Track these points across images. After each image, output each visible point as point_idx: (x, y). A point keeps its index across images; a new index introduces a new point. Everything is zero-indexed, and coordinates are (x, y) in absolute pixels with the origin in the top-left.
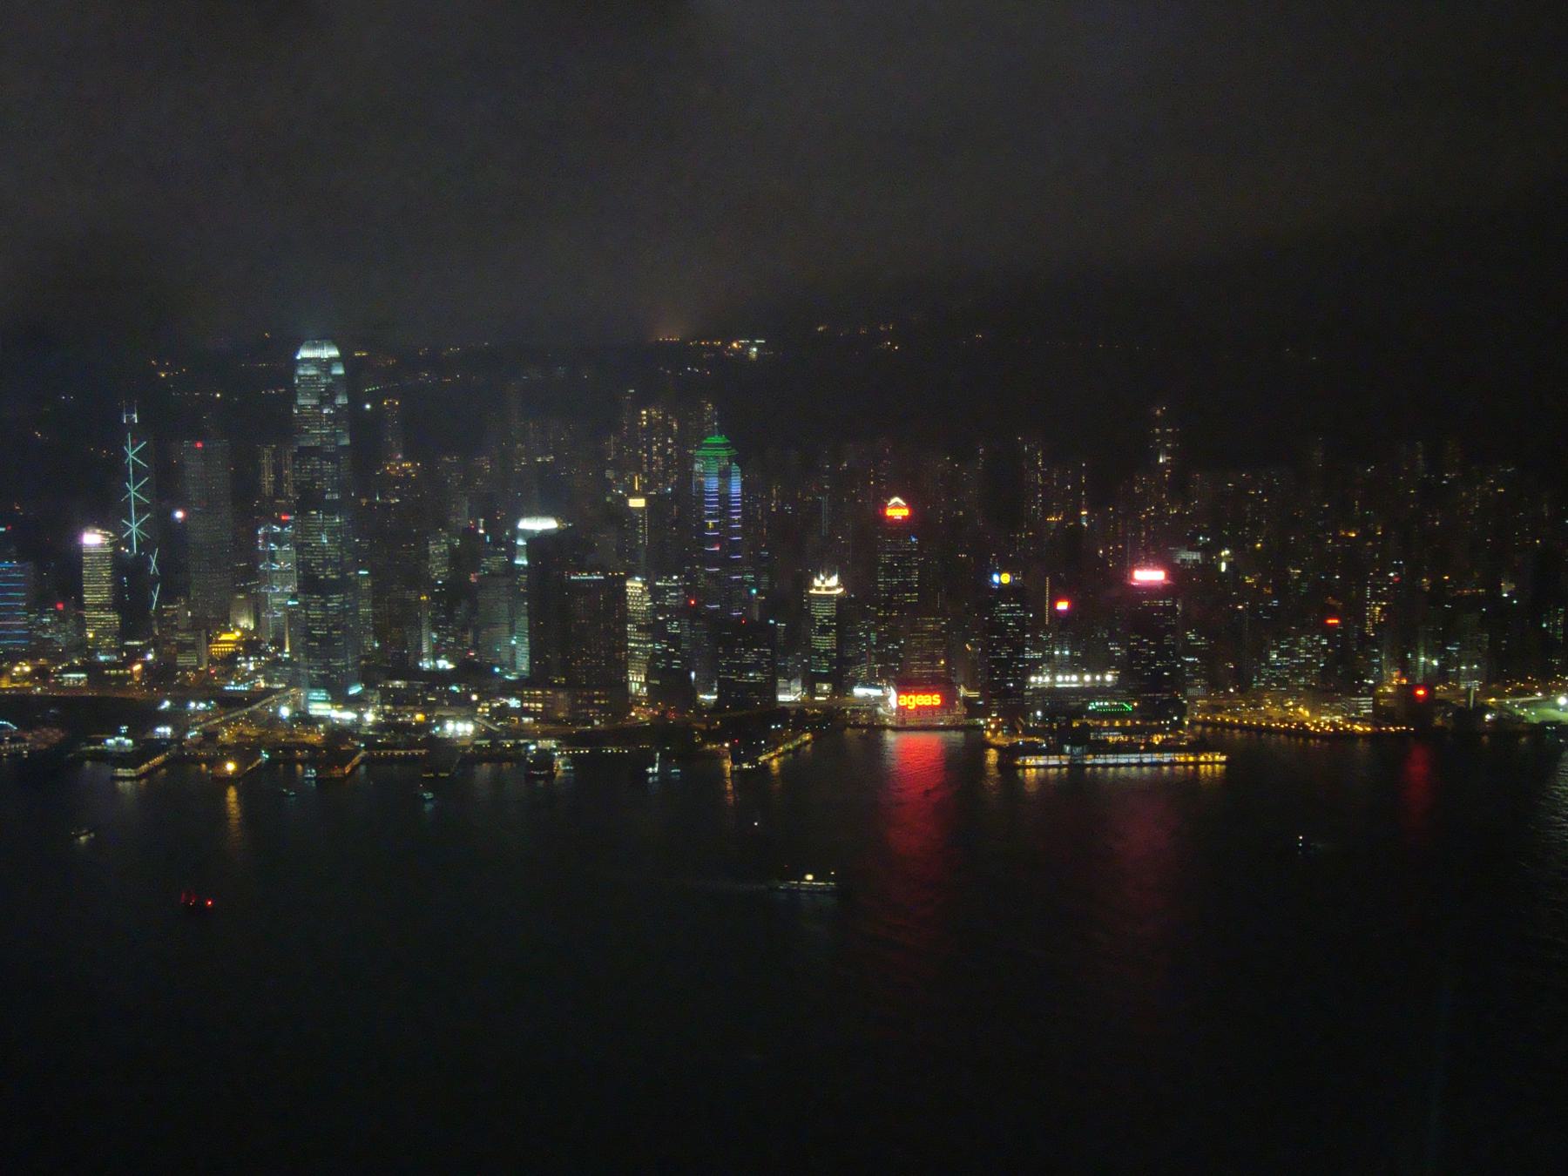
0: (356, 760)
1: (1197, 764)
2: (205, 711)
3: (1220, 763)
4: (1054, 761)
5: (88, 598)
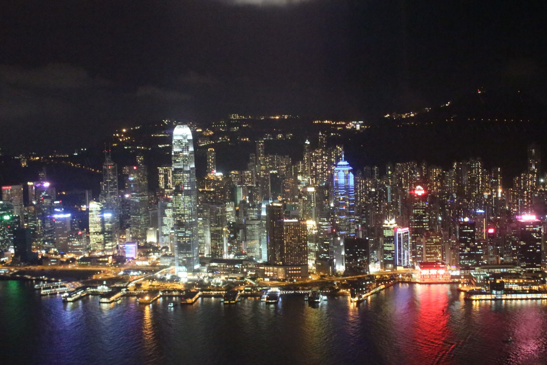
0: (197, 296)
2: (137, 275)
4: (489, 297)
5: (91, 230)
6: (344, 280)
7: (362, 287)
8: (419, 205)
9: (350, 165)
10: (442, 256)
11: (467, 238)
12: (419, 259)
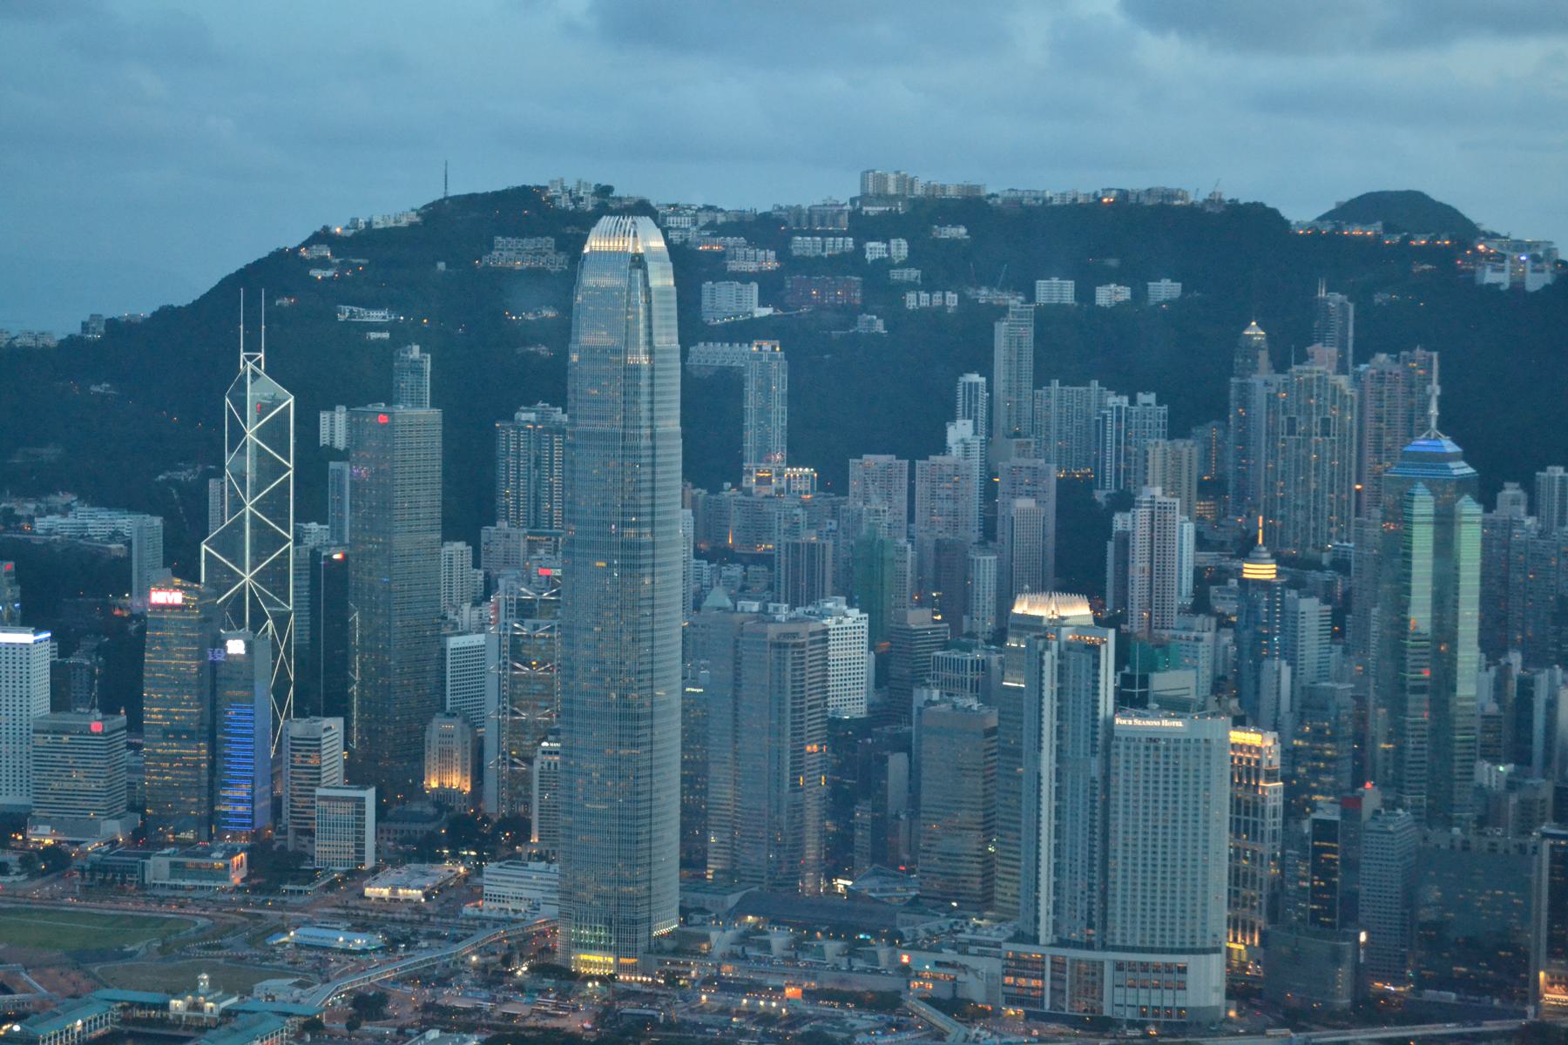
2: (364, 951)
5: (154, 715)
9: (1468, 457)
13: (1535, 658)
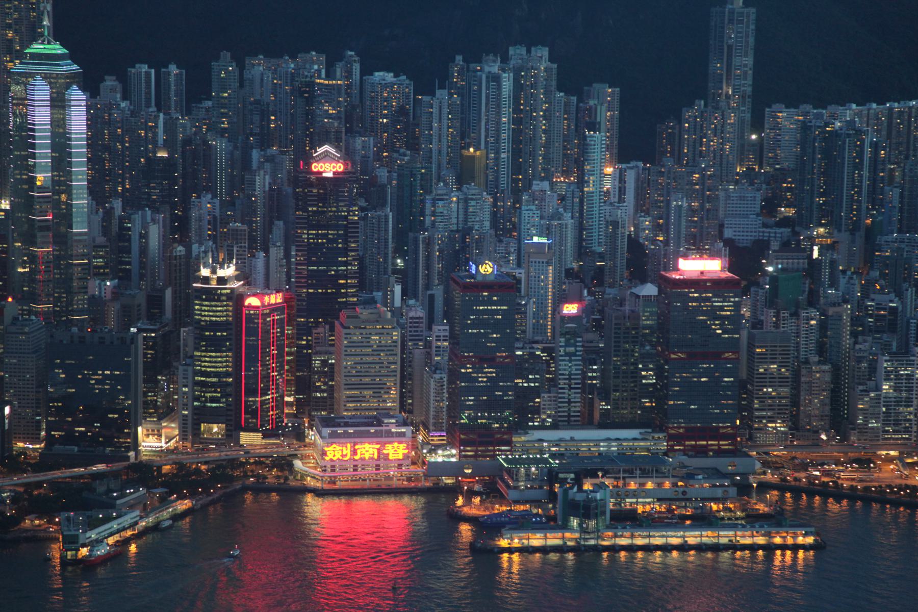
1: (770, 549)
3: (805, 547)
6: (39, 485)
7: (110, 505)
8: (324, 212)
9: (73, 57)
10: (402, 396)
11: (485, 335)
12: (321, 404)
13: (133, 202)
